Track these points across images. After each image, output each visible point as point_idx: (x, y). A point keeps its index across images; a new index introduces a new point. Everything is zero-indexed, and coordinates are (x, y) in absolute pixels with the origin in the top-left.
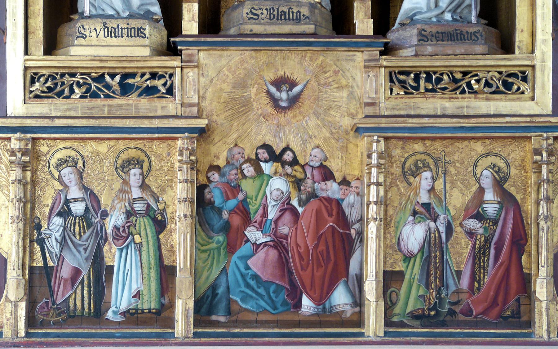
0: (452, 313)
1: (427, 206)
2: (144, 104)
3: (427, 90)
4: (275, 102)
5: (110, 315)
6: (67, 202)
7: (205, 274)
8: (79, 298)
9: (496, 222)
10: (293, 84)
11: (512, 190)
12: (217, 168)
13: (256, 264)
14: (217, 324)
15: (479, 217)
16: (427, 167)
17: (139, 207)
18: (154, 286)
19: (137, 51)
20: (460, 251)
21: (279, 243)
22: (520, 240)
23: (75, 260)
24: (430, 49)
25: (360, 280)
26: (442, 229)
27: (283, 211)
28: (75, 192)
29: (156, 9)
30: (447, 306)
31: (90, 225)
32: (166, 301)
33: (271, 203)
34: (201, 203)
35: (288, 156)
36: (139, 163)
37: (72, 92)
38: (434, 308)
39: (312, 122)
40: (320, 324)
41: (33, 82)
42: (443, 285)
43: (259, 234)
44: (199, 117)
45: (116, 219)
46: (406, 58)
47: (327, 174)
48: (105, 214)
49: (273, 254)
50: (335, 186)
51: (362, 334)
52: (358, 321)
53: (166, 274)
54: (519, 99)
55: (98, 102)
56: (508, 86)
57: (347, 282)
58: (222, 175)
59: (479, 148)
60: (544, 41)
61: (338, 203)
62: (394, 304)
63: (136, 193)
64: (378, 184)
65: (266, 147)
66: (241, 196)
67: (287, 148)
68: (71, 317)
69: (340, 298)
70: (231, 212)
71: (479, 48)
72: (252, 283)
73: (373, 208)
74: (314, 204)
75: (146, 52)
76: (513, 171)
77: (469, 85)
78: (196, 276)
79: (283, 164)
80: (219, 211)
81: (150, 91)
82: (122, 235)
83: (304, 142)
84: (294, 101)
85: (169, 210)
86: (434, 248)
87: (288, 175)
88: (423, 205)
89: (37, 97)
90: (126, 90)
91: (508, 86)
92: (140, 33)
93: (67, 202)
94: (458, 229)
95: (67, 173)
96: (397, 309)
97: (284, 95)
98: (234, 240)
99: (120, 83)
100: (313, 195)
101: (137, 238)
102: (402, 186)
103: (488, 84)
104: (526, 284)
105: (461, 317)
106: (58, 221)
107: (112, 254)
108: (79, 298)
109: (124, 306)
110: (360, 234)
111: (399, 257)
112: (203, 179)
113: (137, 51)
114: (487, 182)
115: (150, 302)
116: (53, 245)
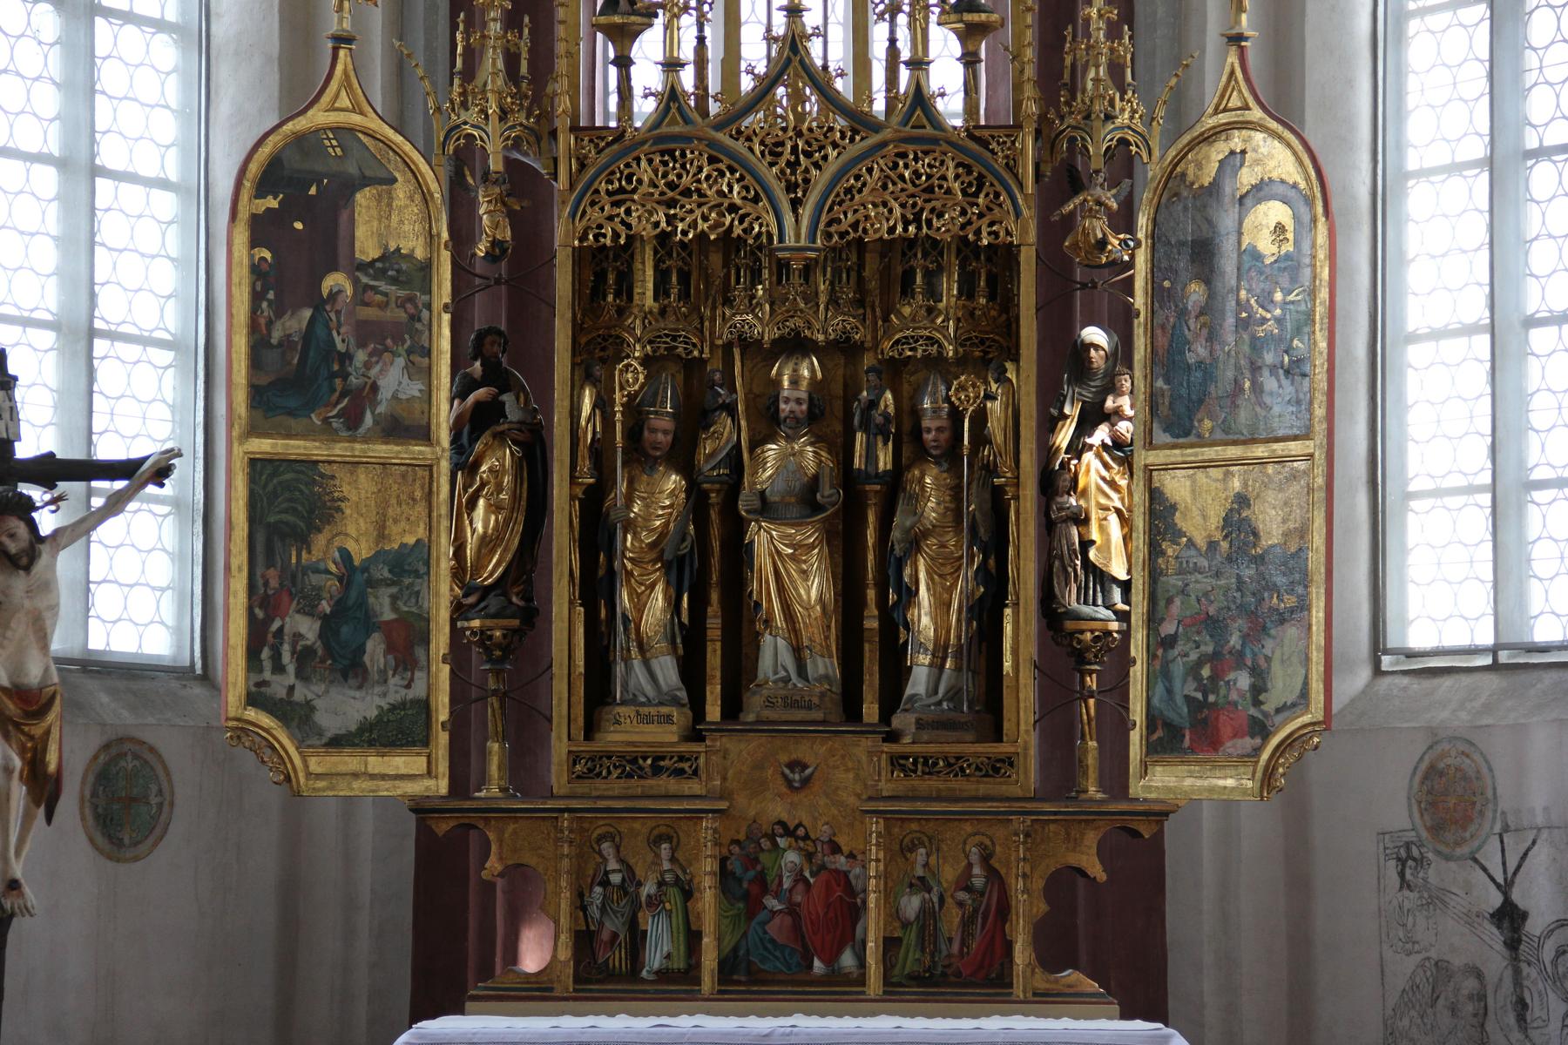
0: (944, 974)
1: (922, 879)
3: (924, 773)
4: (789, 782)
5: (644, 974)
6: (607, 873)
7: (728, 938)
8: (618, 958)
9: (982, 894)
10: (805, 767)
11: (997, 865)
12: (737, 842)
13: (773, 929)
14: (739, 983)
15: (968, 889)
16: (922, 844)
17: (668, 877)
18: (682, 948)
20: (952, 920)
21: (792, 910)
22: (1004, 910)
23: (613, 925)
24: (925, 737)
25: (864, 943)
26: (935, 899)
27: (796, 881)
28: (613, 865)
29: (683, 695)
30: (940, 969)
31: (626, 893)
32: (693, 962)
33: (786, 874)
34: (725, 875)
35: (801, 832)
36: (669, 839)
37: (609, 773)
38: (929, 970)
39: (823, 801)
40: (830, 984)
41: (575, 764)
42: (936, 950)
43: (775, 902)
44: (721, 798)
45: (649, 889)
46: (906, 745)
47: (835, 849)
48: (640, 884)
49: (788, 920)
50: (843, 859)
51: (863, 993)
52: (862, 981)
53: (693, 938)
54: (1005, 783)
55: (634, 782)
56: (997, 770)
57: (853, 947)
58: (742, 848)
59: (968, 828)
60: (1027, 731)
61: (846, 874)
62: (893, 966)
63: (666, 866)
64: (878, 860)
65: (781, 823)
66: (759, 868)
67: (800, 825)
68: (610, 975)
69: (847, 960)
70: (750, 882)
71: (969, 737)
72: (770, 946)
73: (873, 881)
74: (824, 875)
75: (675, 739)
76: (998, 849)
77: (962, 769)
78: (719, 939)
79: (797, 838)
80: (740, 881)
81: (681, 772)
82: (654, 902)
83: (815, 819)
84: (806, 782)
85: (696, 881)
86: (928, 916)
87: (800, 849)
88: (920, 878)
89: (579, 777)
90: (657, 770)
91: (997, 770)
92: (668, 719)
93: (607, 873)
94: (949, 900)
95: (606, 847)
96: (896, 971)
97: (797, 777)
98: (753, 906)
99: (652, 765)
100: (823, 867)
101: (668, 906)
102: (900, 860)
103: (978, 768)
104: (1009, 947)
105: (952, 979)
106: (598, 889)
107: (648, 922)
108: (618, 958)
109: (656, 965)
110: (864, 902)
111: (897, 924)
112: (725, 851)
113: (667, 735)
114: (974, 858)
115: (679, 963)
116: (594, 912)
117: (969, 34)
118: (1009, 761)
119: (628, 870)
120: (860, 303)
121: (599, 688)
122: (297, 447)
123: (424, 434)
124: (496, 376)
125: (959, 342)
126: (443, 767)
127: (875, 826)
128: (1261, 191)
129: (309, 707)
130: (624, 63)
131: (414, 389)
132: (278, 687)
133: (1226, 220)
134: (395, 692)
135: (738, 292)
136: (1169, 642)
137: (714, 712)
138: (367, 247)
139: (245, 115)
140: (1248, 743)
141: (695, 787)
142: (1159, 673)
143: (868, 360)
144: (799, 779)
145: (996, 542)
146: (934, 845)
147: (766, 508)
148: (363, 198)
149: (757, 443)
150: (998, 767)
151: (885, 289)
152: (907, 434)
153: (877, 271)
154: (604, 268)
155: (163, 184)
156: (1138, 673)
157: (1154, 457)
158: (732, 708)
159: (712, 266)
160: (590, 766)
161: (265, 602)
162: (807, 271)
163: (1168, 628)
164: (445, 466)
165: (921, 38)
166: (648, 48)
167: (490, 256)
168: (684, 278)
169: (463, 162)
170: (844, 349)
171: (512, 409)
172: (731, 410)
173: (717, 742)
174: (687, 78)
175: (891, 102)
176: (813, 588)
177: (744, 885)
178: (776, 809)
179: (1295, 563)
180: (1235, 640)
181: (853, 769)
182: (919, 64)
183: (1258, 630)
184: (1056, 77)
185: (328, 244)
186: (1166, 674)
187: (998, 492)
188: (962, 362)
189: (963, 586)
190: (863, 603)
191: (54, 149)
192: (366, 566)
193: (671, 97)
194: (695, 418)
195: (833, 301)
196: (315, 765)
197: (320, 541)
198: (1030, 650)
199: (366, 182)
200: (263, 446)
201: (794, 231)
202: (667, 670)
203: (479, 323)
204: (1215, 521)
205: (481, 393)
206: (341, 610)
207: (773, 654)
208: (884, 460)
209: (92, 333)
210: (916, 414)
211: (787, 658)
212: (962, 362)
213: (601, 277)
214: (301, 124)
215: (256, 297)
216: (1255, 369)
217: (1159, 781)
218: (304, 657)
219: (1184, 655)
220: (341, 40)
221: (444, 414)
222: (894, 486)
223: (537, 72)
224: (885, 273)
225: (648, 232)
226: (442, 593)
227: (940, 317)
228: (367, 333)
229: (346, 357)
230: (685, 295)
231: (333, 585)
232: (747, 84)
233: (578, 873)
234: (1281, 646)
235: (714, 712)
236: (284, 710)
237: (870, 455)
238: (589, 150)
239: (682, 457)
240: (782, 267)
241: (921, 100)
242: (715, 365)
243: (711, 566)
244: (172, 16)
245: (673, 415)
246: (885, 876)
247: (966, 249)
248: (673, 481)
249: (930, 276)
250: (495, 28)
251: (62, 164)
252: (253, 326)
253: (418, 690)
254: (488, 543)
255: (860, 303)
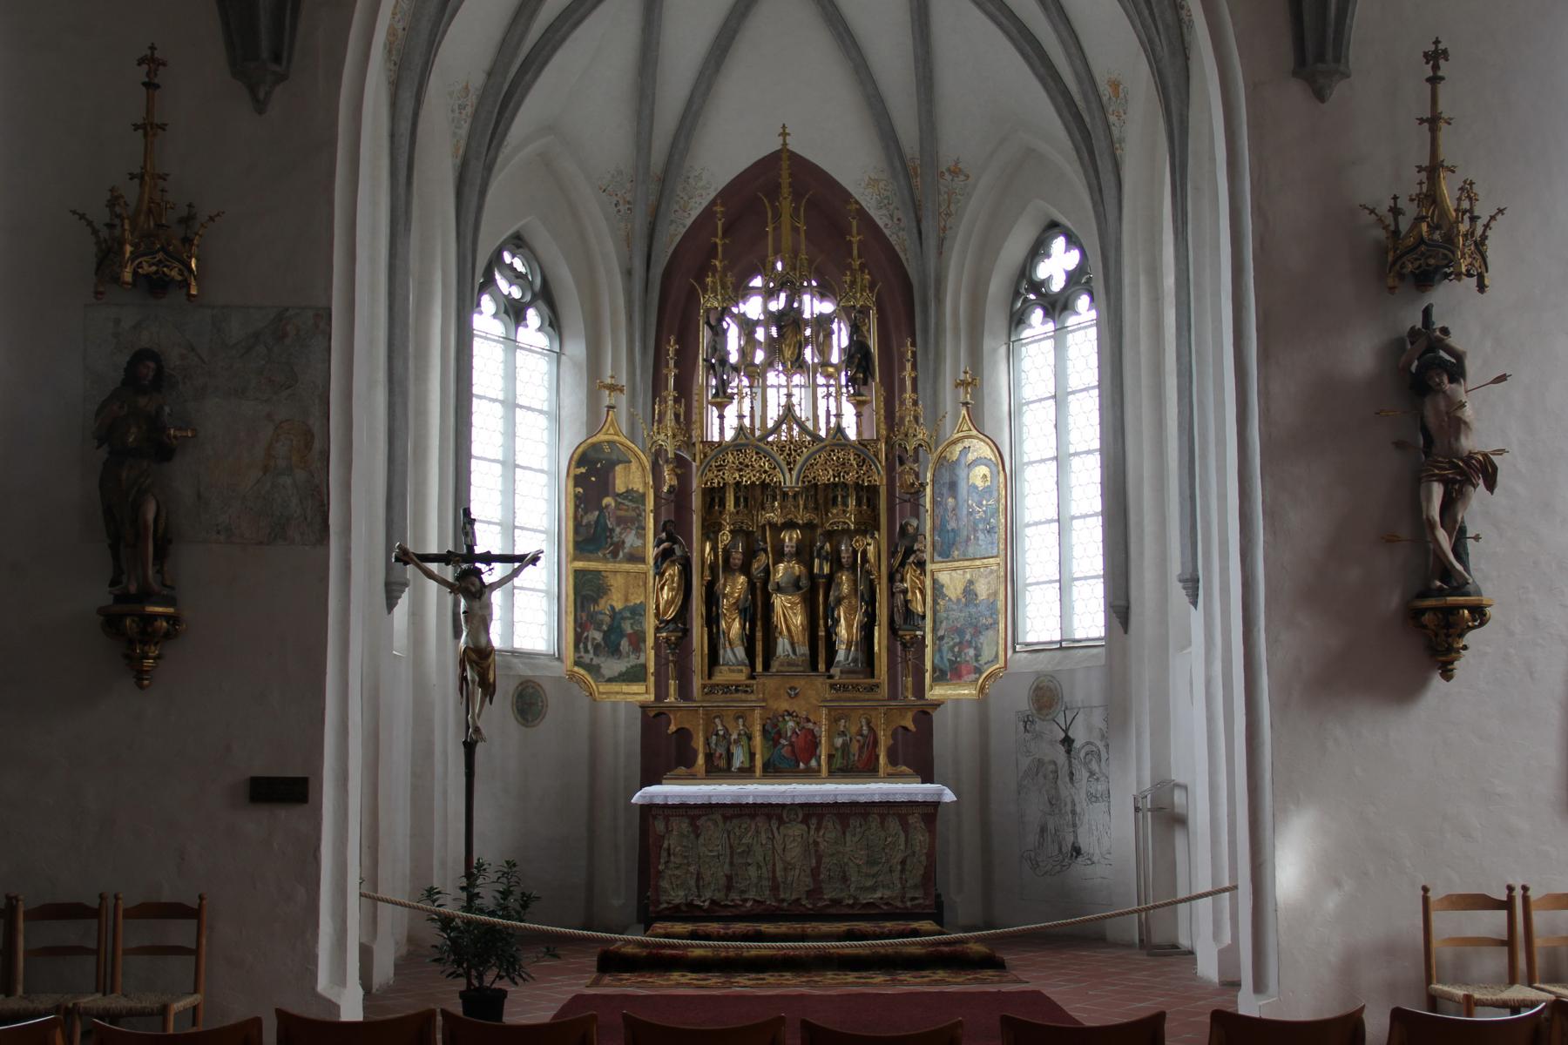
2: (743, 696)
13: (783, 751)
19: (741, 677)
20: (855, 747)
21: (792, 744)
22: (876, 743)
23: (721, 751)
34: (765, 732)
45: (734, 736)
47: (808, 720)
53: (752, 756)
90: (737, 691)
98: (776, 743)
104: (877, 758)
113: (741, 677)
115: (747, 765)
117: (858, 405)
118: (877, 686)
119: (726, 730)
120: (816, 509)
121: (713, 659)
122: (593, 565)
123: (643, 560)
124: (671, 538)
125: (856, 523)
126: (652, 689)
127: (824, 711)
128: (976, 462)
129: (598, 667)
130: (721, 417)
131: (639, 543)
132: (587, 658)
133: (962, 473)
134: (632, 660)
135: (768, 505)
136: (942, 638)
137: (759, 668)
138: (620, 487)
139: (574, 437)
140: (973, 676)
141: (753, 697)
142: (938, 650)
143: (819, 531)
144: (794, 694)
145: (871, 601)
146: (847, 718)
147: (779, 589)
148: (619, 468)
149: (776, 563)
150: (872, 688)
151: (826, 504)
152: (835, 560)
153: (821, 496)
154: (713, 496)
155: (542, 471)
156: (928, 651)
157: (935, 567)
158: (766, 667)
159: (756, 494)
160: (710, 690)
161: (581, 625)
162: (795, 496)
163: (941, 633)
164: (652, 573)
165: (839, 406)
166: (731, 412)
167: (669, 492)
168: (746, 500)
169: (657, 455)
170: (809, 527)
171: (678, 552)
172: (765, 551)
173: (761, 680)
174: (747, 422)
175: (828, 430)
176: (798, 620)
177: (772, 734)
178: (784, 705)
179: (992, 607)
180: (968, 637)
181: (815, 690)
182: (839, 416)
183: (978, 632)
184: (891, 418)
185: (605, 486)
186: (940, 650)
187: (872, 581)
188: (857, 532)
189: (858, 618)
190: (818, 625)
191: (500, 457)
192: (621, 612)
193: (740, 429)
194: (750, 554)
195: (805, 507)
196: (602, 689)
197: (602, 602)
198: (885, 642)
199: (620, 462)
200: (580, 565)
201: (789, 480)
202: (740, 652)
203: (663, 519)
204: (959, 591)
205: (666, 545)
206: (611, 628)
207: (783, 645)
208: (826, 570)
209: (515, 527)
210: (838, 552)
211: (788, 647)
212: (857, 532)
213: (713, 499)
214: (594, 440)
215: (577, 507)
216: (975, 531)
217: (936, 692)
218: (597, 647)
219: (946, 644)
220: (610, 407)
221: (651, 553)
222: (830, 579)
223: (687, 422)
224: (826, 497)
225: (731, 481)
226: (650, 623)
227: (847, 514)
228: (621, 521)
229: (612, 530)
230: (746, 506)
231: (608, 619)
232: (770, 424)
233: (706, 731)
234: (985, 639)
235: (759, 668)
236: (589, 668)
237: (821, 568)
238: (708, 450)
239: (745, 569)
240: (785, 495)
241: (839, 429)
242: (758, 535)
243: (758, 612)
244: (545, 408)
245: (743, 553)
246: (829, 731)
247: (858, 487)
248: (742, 579)
249: (845, 498)
250: (671, 403)
251: (503, 463)
252: (575, 518)
253: (642, 660)
254: (669, 603)
255: (816, 509)
